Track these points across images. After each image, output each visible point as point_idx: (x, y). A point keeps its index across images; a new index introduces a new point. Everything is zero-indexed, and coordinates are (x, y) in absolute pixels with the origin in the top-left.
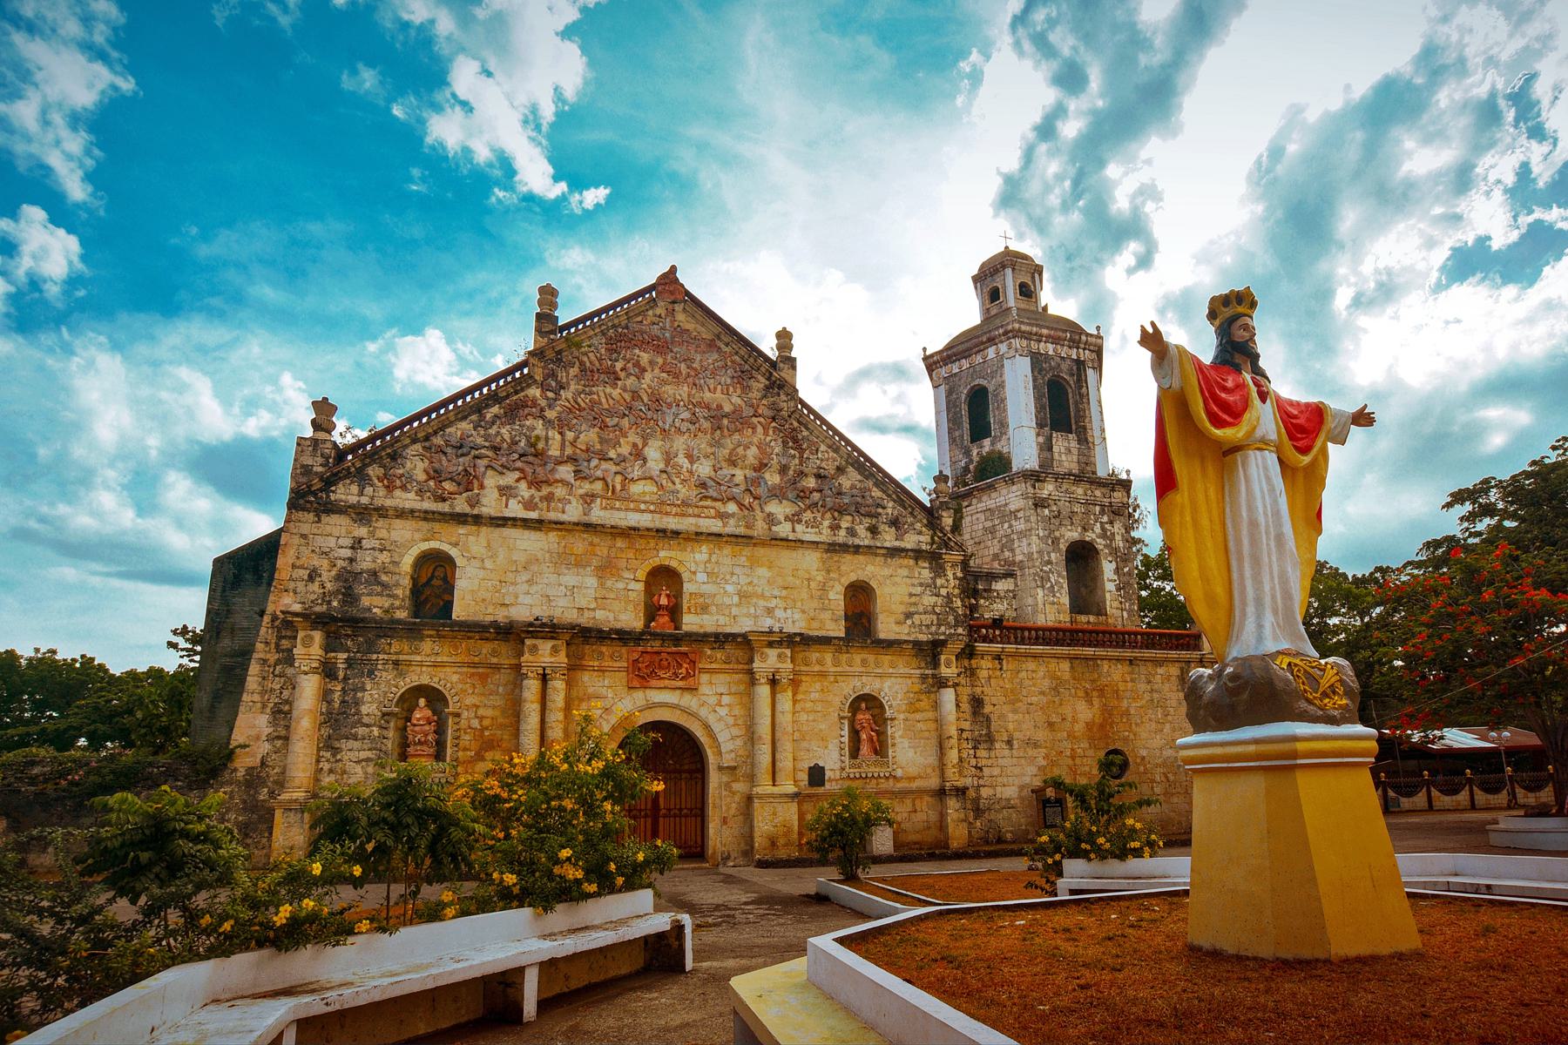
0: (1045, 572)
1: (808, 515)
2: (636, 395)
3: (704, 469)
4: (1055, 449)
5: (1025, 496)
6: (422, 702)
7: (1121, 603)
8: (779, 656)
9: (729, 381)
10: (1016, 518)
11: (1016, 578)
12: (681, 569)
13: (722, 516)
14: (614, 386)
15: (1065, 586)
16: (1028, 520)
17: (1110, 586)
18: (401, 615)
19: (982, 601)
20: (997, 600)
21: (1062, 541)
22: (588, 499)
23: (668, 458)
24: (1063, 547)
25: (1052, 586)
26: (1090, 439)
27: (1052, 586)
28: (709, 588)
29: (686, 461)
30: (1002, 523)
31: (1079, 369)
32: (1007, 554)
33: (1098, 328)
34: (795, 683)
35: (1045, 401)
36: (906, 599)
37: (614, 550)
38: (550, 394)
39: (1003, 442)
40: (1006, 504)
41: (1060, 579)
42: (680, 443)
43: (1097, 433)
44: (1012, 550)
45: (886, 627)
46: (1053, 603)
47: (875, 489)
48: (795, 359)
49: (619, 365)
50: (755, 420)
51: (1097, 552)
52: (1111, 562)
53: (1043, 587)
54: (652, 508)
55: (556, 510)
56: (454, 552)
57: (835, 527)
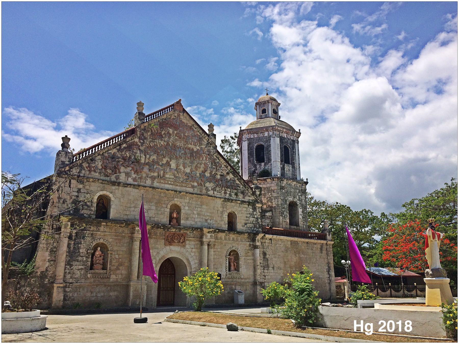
0: (283, 211)
1: (218, 189)
2: (168, 144)
3: (188, 170)
4: (285, 169)
5: (277, 185)
6: (99, 249)
7: (303, 222)
8: (211, 236)
9: (196, 141)
10: (274, 192)
11: (273, 212)
12: (180, 205)
13: (193, 187)
14: (162, 140)
15: (288, 216)
16: (278, 193)
17: (300, 217)
20: (267, 219)
21: (288, 201)
22: (153, 178)
23: (177, 166)
24: (288, 203)
25: (285, 216)
26: (296, 167)
27: (285, 216)
29: (183, 168)
30: (268, 193)
31: (293, 143)
32: (269, 203)
33: (299, 130)
35: (283, 153)
36: (246, 219)
37: (160, 197)
38: (142, 141)
39: (269, 165)
40: (270, 187)
41: (287, 214)
42: (181, 161)
43: (297, 165)
44: (272, 202)
45: (239, 226)
46: (285, 222)
47: (237, 181)
48: (215, 135)
49: (163, 133)
50: (203, 155)
51: (297, 205)
52: (301, 209)
53: (282, 216)
54: (172, 183)
56: (111, 195)
57: (225, 193)
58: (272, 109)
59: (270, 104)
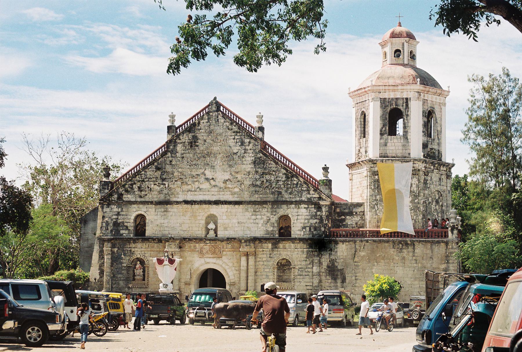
6: (138, 262)
12: (217, 215)
13: (233, 194)
18: (132, 236)
19: (348, 217)
25: (376, 211)
28: (227, 221)
34: (255, 254)
35: (387, 121)
45: (296, 231)
55: (176, 197)
58: (392, 52)
59: (390, 44)
